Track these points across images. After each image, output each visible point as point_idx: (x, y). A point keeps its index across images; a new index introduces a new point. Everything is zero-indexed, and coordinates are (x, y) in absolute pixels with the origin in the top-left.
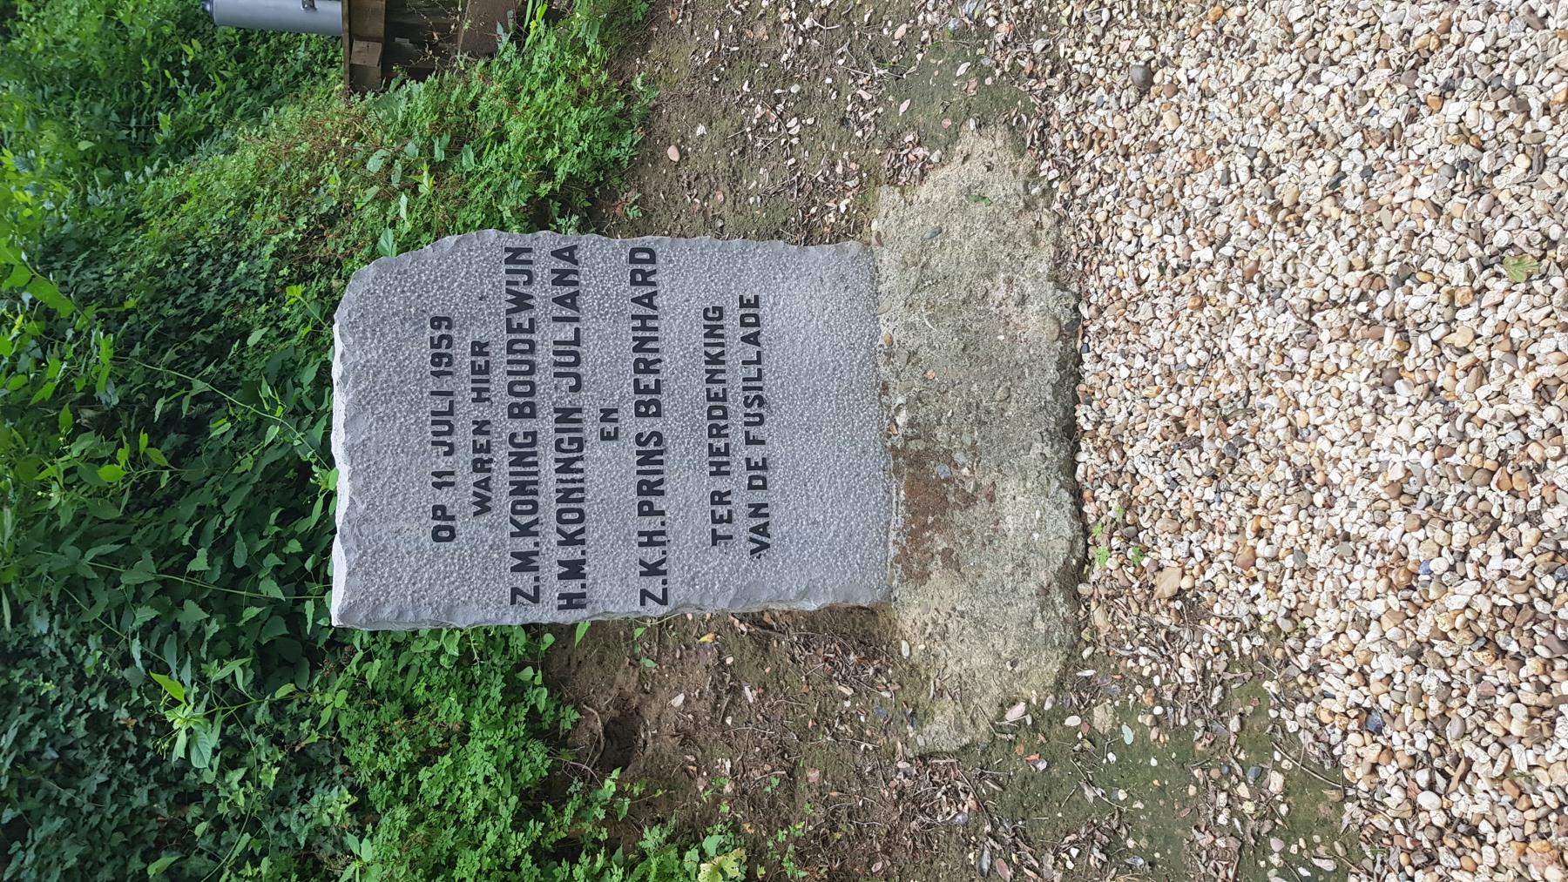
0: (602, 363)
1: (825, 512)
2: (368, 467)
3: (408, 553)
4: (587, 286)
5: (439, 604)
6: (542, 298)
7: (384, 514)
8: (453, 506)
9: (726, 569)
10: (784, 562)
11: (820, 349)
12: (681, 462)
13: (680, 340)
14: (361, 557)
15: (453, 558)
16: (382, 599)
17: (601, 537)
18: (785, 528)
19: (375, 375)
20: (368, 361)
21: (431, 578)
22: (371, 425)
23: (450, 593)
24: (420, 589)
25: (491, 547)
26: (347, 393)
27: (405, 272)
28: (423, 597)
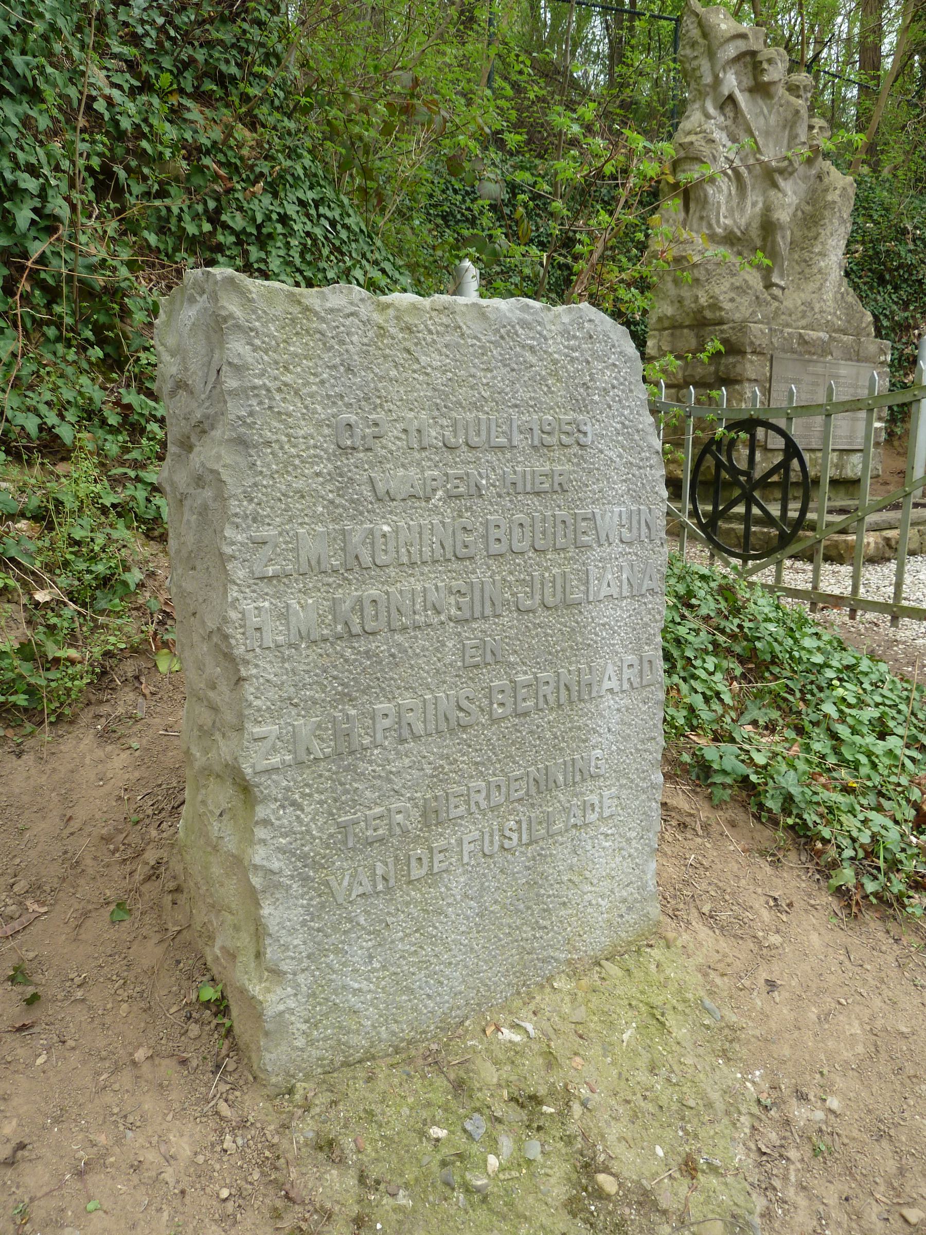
0: (546, 635)
1: (384, 968)
2: (430, 332)
3: (322, 382)
4: (621, 608)
5: (250, 426)
6: (610, 554)
7: (372, 349)
8: (383, 447)
9: (306, 849)
10: (319, 930)
11: (564, 904)
12: (442, 757)
13: (571, 729)
14: (316, 314)
15: (315, 447)
16: (257, 342)
17: (346, 661)
18: (362, 920)
19: (531, 348)
20: (546, 339)
21: (289, 415)
22: (479, 340)
23: (268, 443)
24: (271, 399)
25: (332, 502)
26: (511, 310)
27: (631, 391)
28: (261, 403)
